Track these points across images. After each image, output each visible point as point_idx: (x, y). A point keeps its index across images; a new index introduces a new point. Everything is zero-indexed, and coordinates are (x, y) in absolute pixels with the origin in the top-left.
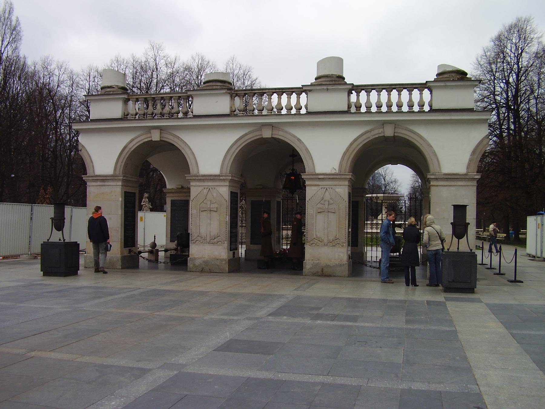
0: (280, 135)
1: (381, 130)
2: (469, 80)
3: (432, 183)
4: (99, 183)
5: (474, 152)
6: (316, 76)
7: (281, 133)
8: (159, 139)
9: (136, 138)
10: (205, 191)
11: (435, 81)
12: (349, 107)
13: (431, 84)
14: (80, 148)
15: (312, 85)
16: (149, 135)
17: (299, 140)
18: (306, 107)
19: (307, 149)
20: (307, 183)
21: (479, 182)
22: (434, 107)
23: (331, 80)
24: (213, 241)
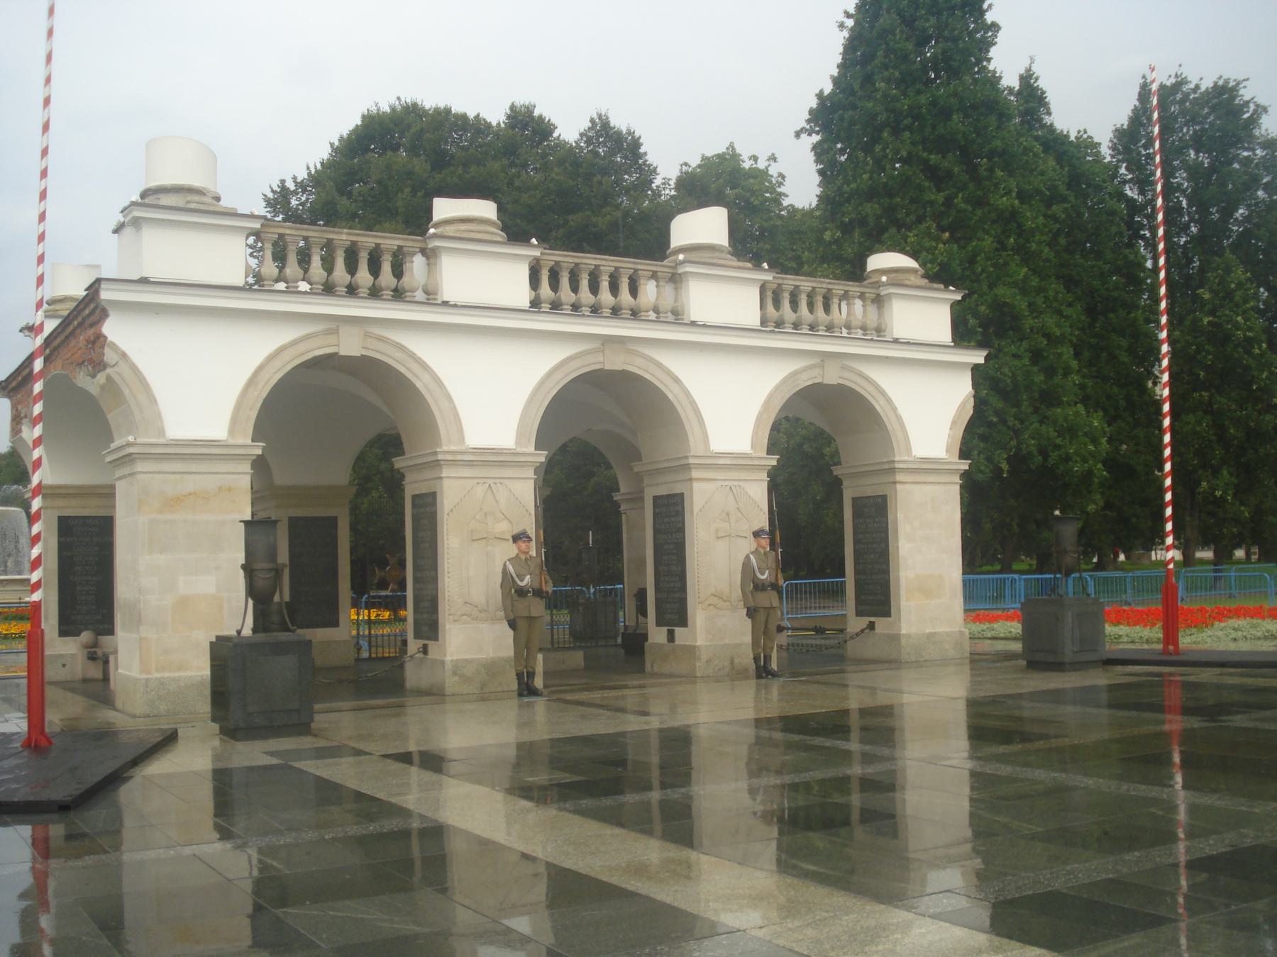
0: (635, 366)
1: (816, 372)
3: (899, 477)
5: (954, 423)
7: (638, 361)
9: (293, 343)
10: (480, 491)
14: (109, 356)
16: (331, 339)
17: (677, 380)
19: (693, 403)
20: (695, 474)
21: (965, 475)
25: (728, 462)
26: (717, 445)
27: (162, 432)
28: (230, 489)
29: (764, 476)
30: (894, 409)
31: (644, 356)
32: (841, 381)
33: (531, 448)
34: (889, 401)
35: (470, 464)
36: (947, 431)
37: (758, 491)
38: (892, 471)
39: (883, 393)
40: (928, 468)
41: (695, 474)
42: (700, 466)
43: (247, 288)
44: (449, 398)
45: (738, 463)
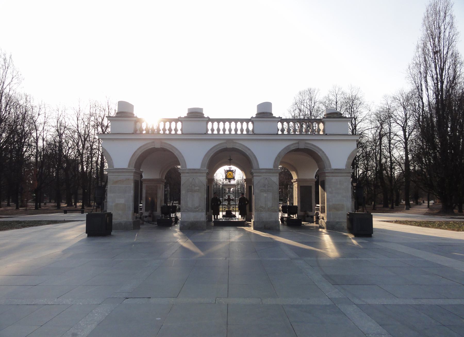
1: (297, 145)
2: (275, 117)
3: (327, 174)
4: (117, 174)
6: (256, 113)
8: (159, 147)
10: (191, 180)
11: (255, 117)
12: (207, 130)
13: (252, 120)
15: (185, 117)
17: (249, 149)
18: (181, 130)
19: (254, 155)
20: (254, 174)
22: (326, 133)
23: (196, 115)
24: (195, 210)
25: (265, 171)
26: (261, 167)
27: (113, 167)
28: (128, 179)
29: (278, 174)
30: (325, 154)
31: (239, 143)
32: (306, 147)
33: (206, 169)
34: (323, 152)
35: (188, 173)
36: (346, 160)
37: (275, 179)
38: (325, 173)
39: (321, 150)
40: (338, 172)
41: (327, 174)
42: (257, 172)
43: (133, 134)
44: (183, 157)
45: (268, 171)
